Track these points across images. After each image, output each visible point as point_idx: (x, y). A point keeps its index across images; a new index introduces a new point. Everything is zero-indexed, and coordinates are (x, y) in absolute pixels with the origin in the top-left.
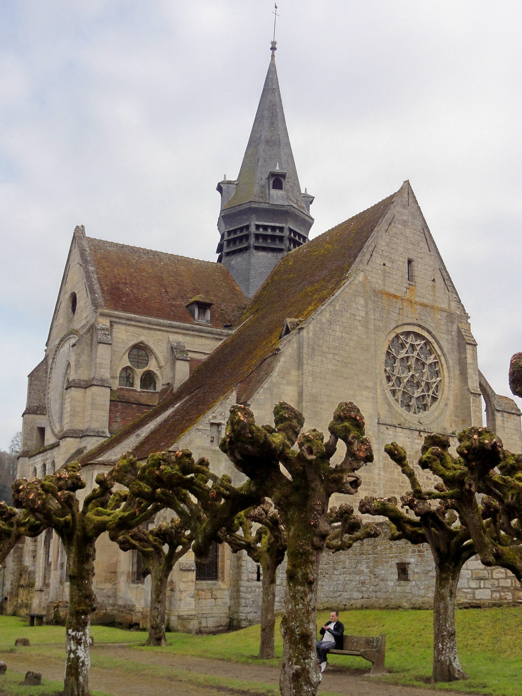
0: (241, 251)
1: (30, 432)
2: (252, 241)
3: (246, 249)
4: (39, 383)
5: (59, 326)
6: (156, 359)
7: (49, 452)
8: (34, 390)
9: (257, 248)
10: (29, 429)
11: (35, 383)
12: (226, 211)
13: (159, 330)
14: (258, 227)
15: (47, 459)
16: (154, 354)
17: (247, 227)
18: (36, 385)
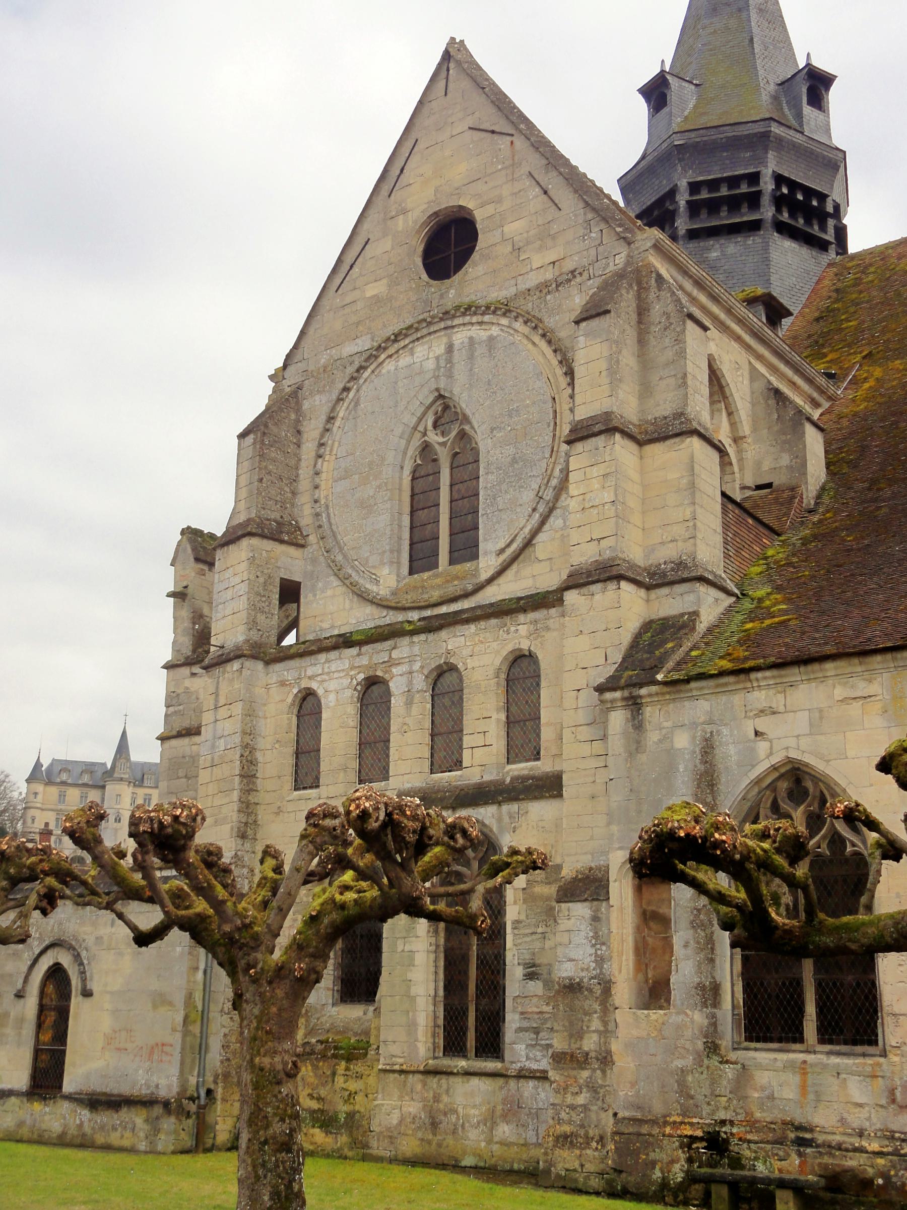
0: (734, 230)
1: (265, 590)
2: (767, 212)
3: (755, 226)
4: (280, 457)
5: (360, 305)
6: (730, 414)
7: (406, 641)
8: (269, 473)
9: (781, 228)
10: (261, 580)
11: (273, 455)
12: (693, 135)
13: (738, 339)
14: (779, 179)
15: (391, 663)
16: (725, 397)
17: (754, 178)
18: (274, 460)
